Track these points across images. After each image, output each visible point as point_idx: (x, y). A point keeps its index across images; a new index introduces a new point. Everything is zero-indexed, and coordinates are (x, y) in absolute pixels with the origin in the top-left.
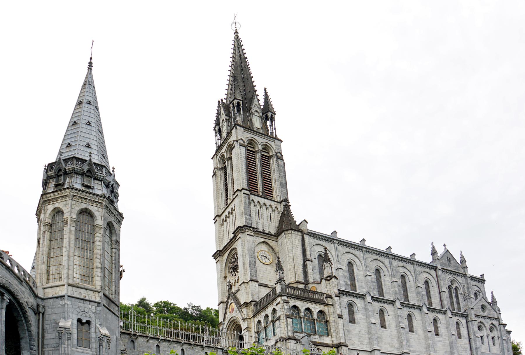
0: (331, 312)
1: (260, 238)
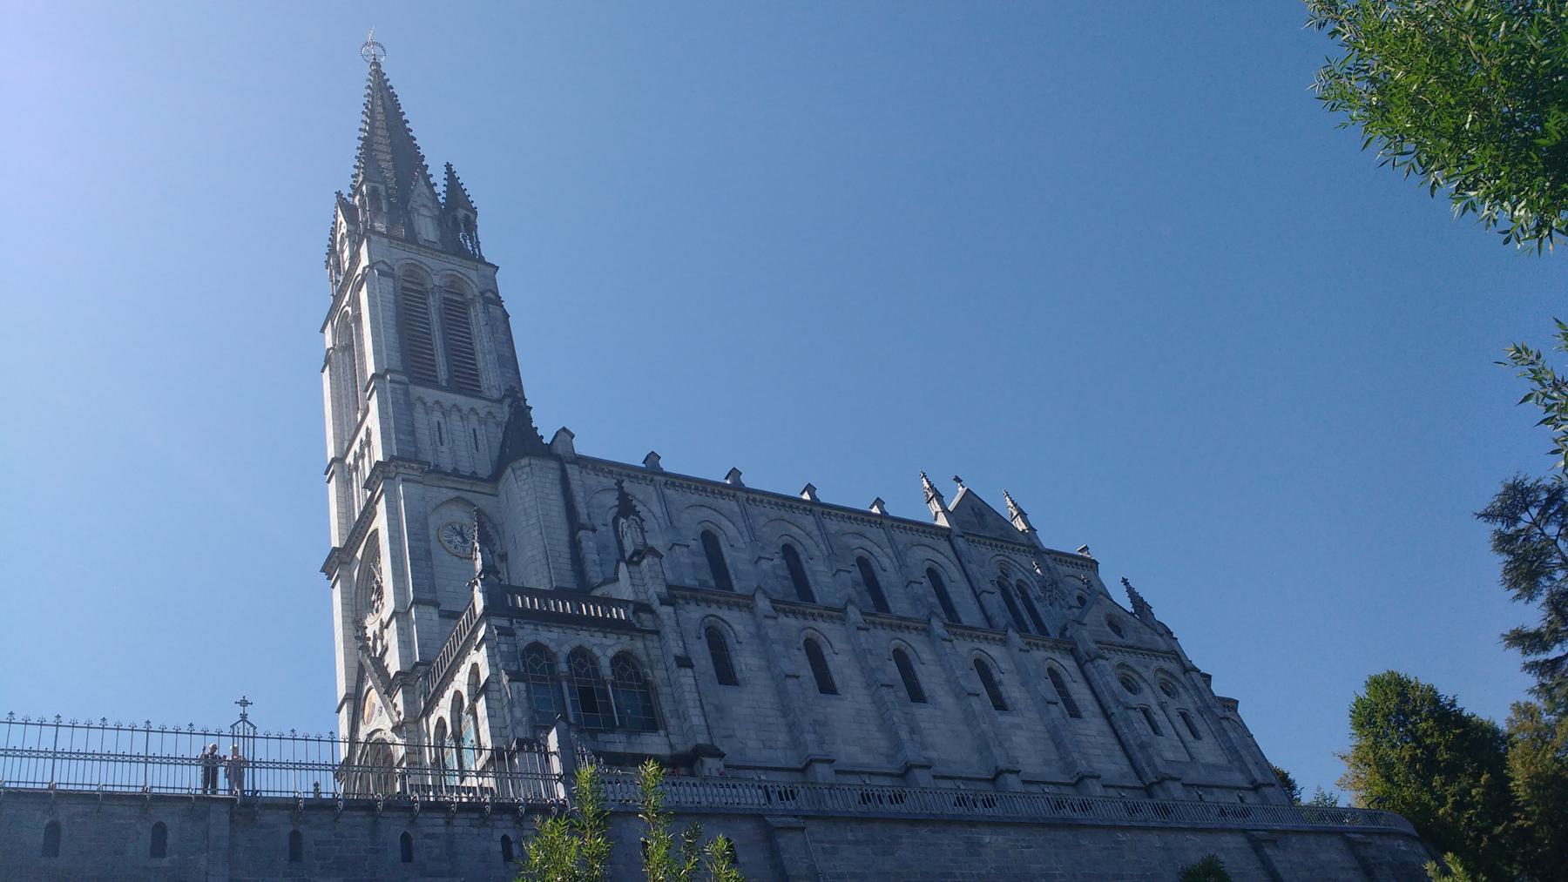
0: (656, 653)
1: (445, 490)
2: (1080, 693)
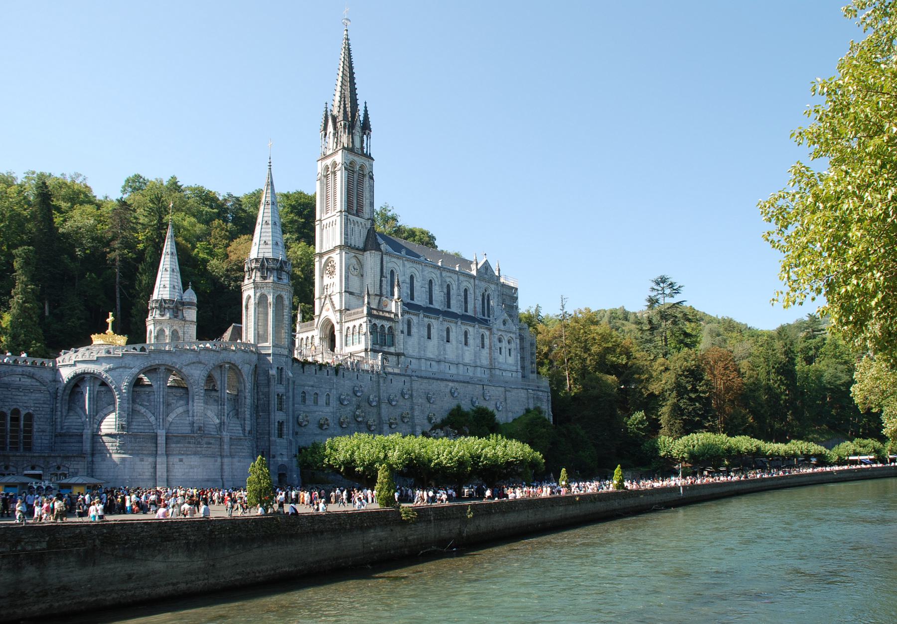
2: (487, 341)
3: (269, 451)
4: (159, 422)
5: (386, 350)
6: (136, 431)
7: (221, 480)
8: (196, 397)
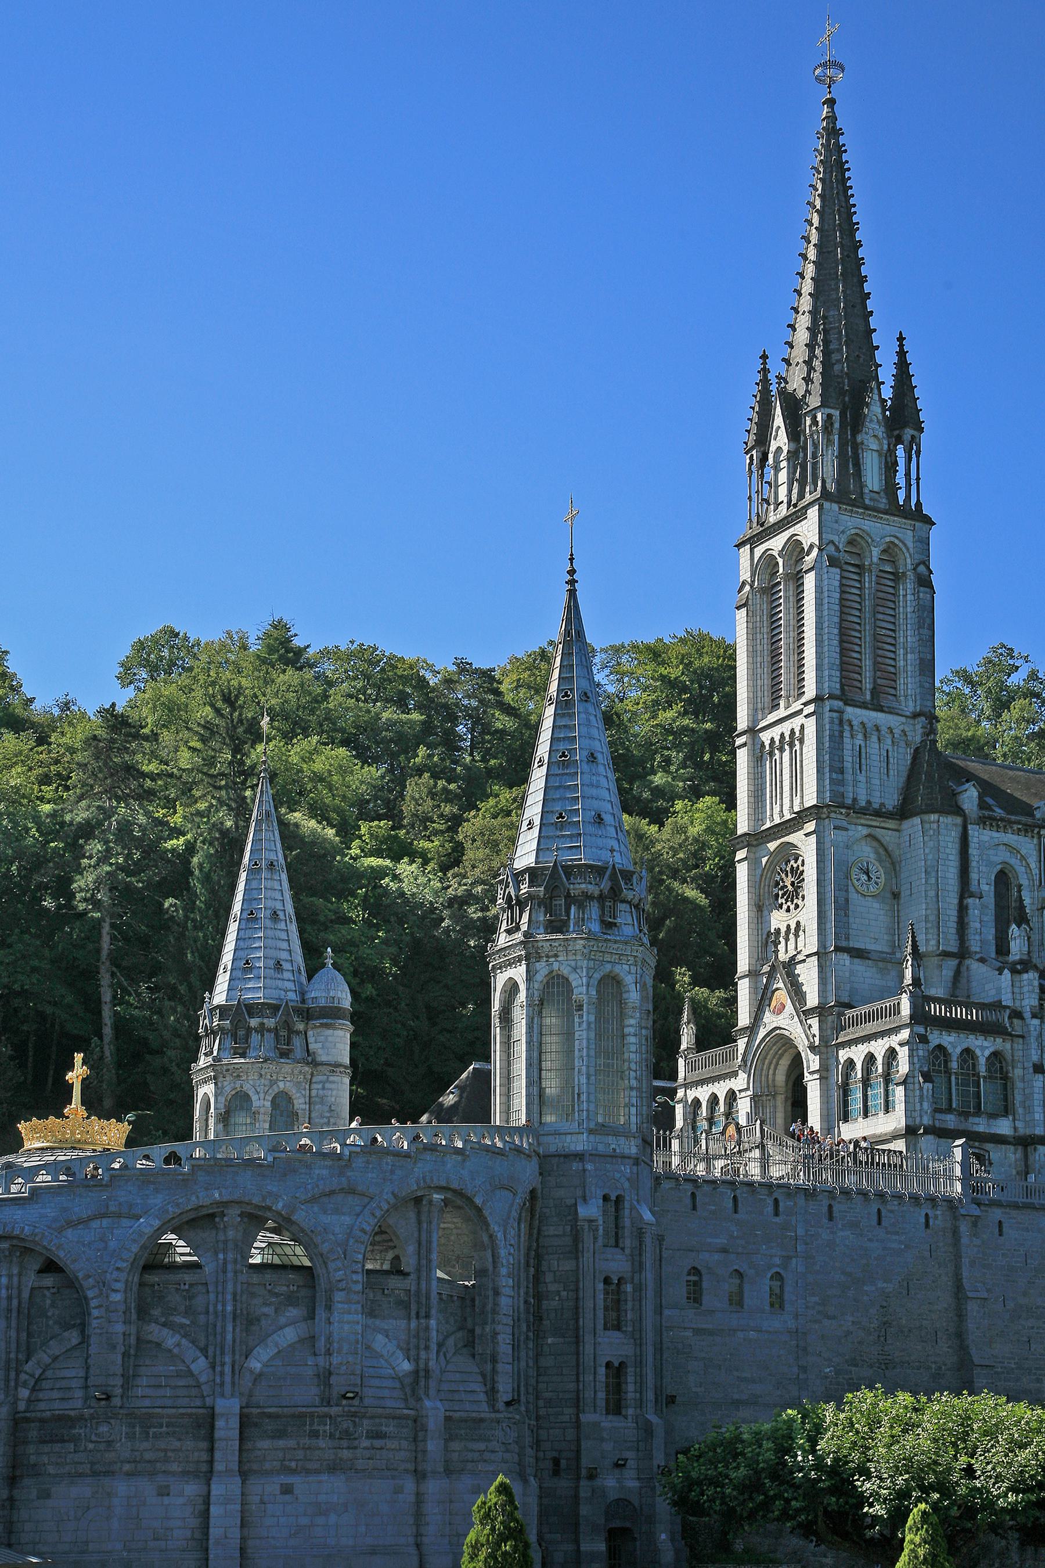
3: (578, 1458)
4: (222, 1374)
5: (981, 1128)
6: (147, 1403)
7: (413, 1550)
8: (339, 1296)
